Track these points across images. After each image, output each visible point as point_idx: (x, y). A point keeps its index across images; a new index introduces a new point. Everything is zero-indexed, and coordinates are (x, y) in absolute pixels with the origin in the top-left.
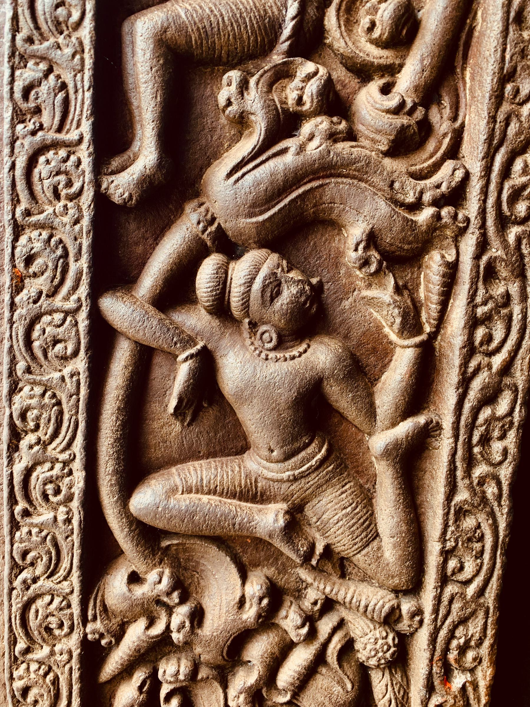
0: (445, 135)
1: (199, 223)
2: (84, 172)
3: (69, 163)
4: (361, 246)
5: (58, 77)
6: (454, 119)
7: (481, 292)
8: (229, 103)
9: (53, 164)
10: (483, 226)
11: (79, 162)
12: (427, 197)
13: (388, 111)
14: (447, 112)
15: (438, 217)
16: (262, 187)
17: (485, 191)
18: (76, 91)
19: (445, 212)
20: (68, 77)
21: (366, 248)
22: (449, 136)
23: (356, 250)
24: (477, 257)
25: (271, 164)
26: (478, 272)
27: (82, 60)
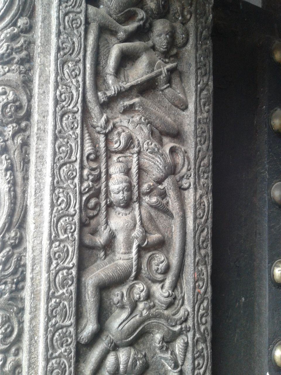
0: (180, 299)
1: (109, 344)
2: (72, 336)
3: (67, 333)
4: (161, 343)
5: (63, 304)
6: (182, 292)
7: (196, 350)
8: (118, 303)
9: (61, 335)
10: (194, 329)
11: (70, 333)
12: (178, 322)
13: (165, 297)
14: (180, 290)
15: (182, 328)
16: (130, 330)
17: (194, 318)
18: (70, 308)
19: (183, 326)
20: (66, 303)
21: (162, 343)
22: (181, 299)
23: (159, 344)
24: (194, 338)
25: (132, 320)
26: (194, 344)
27: (72, 298)
